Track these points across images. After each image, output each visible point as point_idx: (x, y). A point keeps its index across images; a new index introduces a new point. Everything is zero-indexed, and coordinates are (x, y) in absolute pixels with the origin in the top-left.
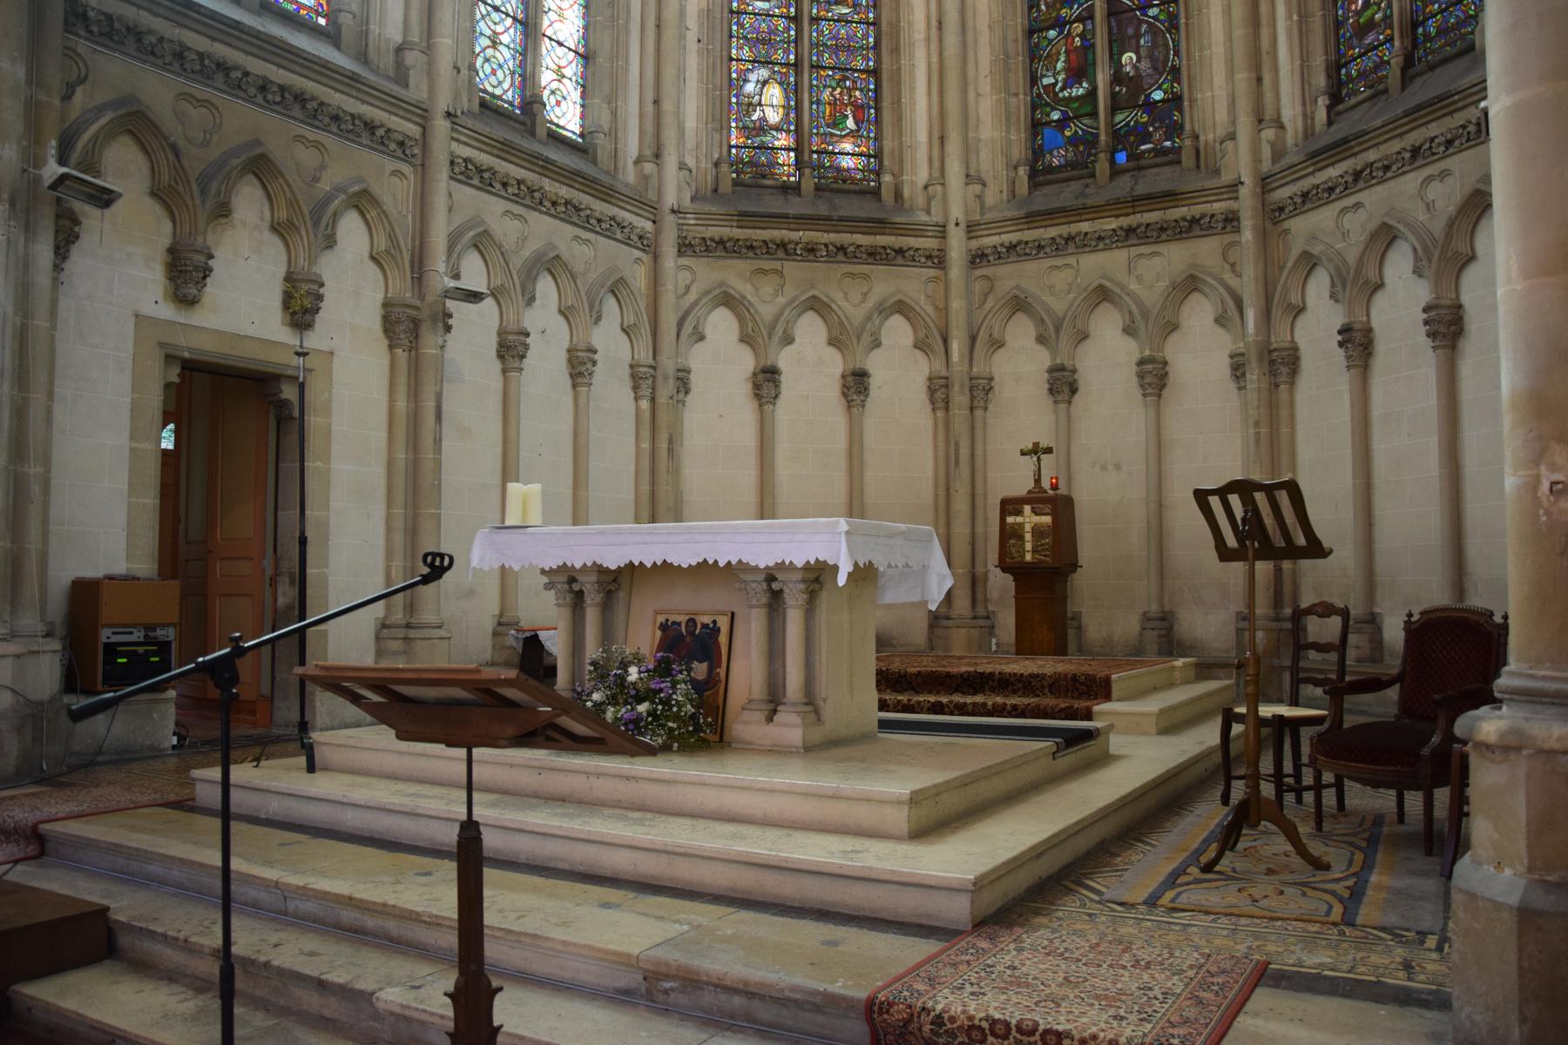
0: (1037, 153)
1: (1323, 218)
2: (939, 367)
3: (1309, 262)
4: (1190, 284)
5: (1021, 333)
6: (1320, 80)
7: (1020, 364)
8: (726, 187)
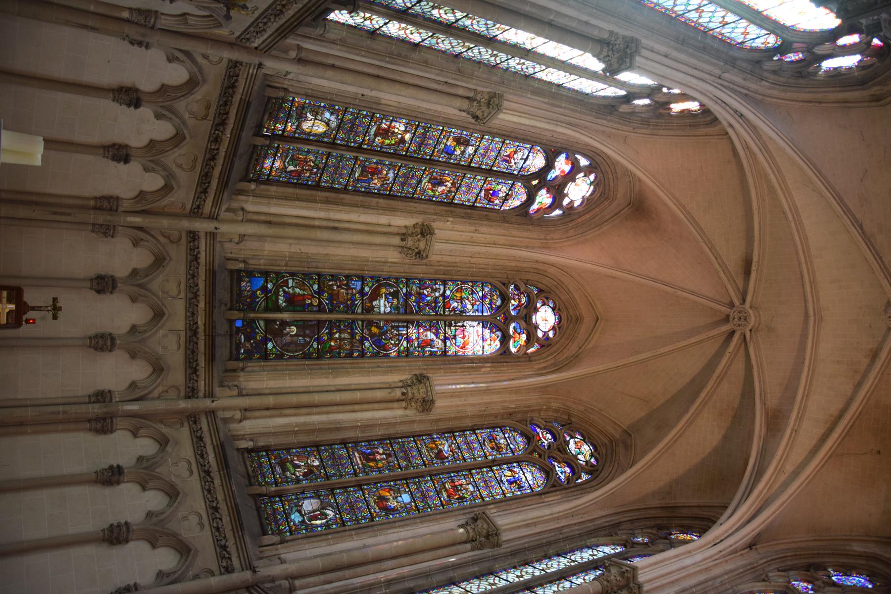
0: (250, 274)
1: (187, 451)
2: (126, 205)
3: (163, 442)
4: (158, 369)
5: (141, 258)
6: (261, 443)
7: (121, 257)
8: (270, 93)
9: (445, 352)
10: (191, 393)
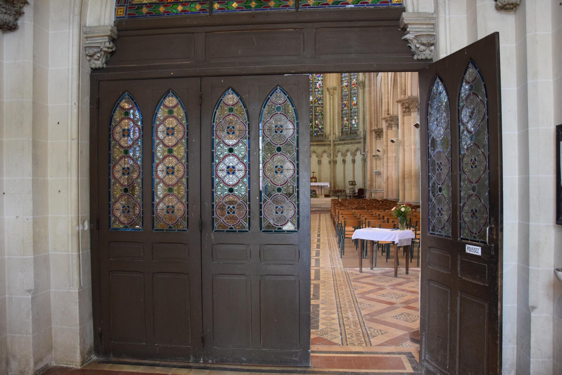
1: (341, 147)
3: (339, 151)
4: (325, 152)
9: (322, 80)
10: (330, 145)
